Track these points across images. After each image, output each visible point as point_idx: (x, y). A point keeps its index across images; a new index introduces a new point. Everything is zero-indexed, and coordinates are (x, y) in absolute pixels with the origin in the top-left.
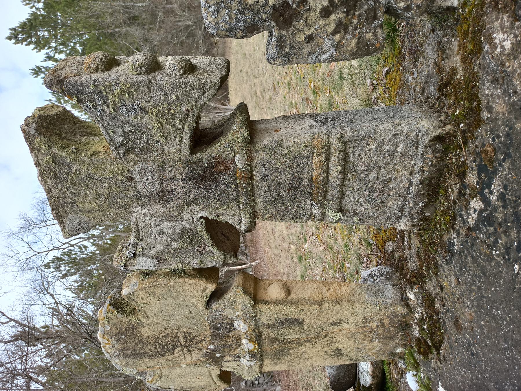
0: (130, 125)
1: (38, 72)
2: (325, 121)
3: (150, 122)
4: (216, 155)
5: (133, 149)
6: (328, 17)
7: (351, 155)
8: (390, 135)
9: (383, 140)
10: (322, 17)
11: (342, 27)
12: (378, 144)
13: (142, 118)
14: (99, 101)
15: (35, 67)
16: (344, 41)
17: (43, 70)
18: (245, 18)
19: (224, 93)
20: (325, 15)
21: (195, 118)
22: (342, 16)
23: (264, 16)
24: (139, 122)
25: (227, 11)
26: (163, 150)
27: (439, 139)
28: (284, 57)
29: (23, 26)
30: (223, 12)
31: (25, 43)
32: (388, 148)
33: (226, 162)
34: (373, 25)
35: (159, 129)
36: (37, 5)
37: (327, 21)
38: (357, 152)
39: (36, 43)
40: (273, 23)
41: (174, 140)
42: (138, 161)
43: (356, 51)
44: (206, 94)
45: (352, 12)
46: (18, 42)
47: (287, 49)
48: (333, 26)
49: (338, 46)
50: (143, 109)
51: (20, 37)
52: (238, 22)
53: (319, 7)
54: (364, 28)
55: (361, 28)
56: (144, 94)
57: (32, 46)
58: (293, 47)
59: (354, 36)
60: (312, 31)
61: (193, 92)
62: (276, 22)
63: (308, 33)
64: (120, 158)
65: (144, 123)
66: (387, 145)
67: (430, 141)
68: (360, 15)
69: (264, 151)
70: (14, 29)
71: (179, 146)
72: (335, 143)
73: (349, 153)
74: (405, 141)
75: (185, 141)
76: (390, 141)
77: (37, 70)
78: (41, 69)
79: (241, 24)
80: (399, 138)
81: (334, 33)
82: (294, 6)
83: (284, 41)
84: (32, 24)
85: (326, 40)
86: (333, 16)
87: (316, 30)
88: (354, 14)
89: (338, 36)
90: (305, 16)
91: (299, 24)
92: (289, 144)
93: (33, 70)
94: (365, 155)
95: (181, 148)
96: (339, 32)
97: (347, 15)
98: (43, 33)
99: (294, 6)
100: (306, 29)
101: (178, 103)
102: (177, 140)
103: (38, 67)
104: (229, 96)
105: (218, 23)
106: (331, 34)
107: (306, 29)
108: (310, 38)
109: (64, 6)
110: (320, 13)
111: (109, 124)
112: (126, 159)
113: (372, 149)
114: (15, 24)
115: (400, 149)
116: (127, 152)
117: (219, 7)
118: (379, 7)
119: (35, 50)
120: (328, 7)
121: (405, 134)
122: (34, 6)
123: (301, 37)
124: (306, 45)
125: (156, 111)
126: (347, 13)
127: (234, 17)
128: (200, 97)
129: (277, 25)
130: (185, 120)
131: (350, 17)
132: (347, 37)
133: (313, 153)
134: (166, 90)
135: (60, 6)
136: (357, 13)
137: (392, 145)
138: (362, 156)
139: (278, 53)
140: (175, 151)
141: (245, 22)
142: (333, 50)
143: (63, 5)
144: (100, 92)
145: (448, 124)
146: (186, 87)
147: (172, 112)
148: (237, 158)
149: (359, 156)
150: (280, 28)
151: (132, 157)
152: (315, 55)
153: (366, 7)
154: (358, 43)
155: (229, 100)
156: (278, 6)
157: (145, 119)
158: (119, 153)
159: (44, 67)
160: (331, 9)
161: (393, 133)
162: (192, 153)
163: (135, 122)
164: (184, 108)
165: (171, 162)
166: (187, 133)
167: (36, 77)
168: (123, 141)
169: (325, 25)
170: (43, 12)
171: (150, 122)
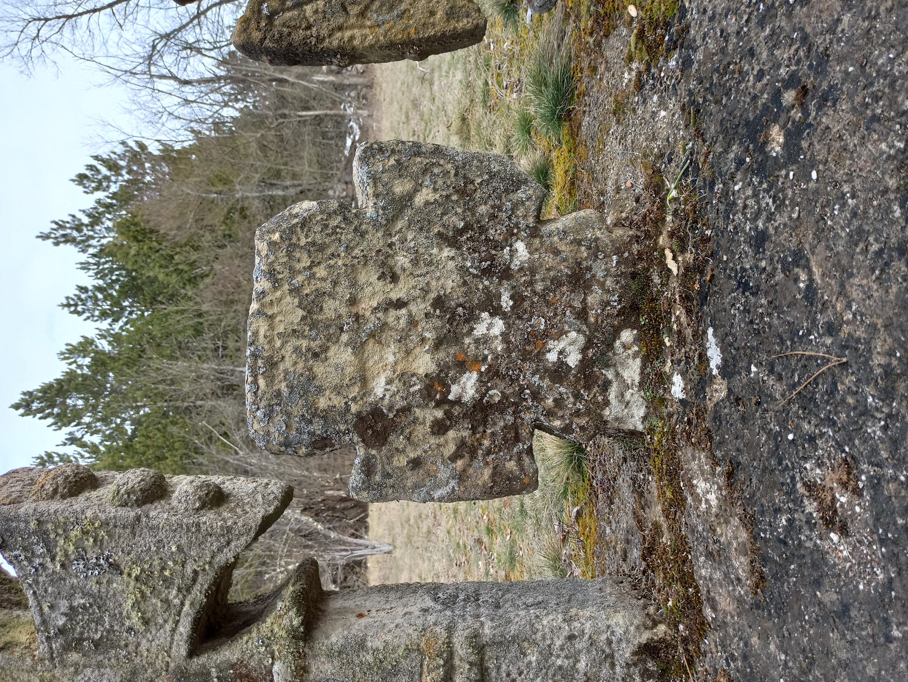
0: (84, 595)
1: (46, 461)
2: (450, 602)
3: (124, 591)
4: (238, 659)
5: (80, 640)
6: (444, 434)
7: (494, 674)
8: (562, 638)
9: (549, 646)
10: (433, 433)
11: (465, 450)
12: (541, 653)
13: (109, 582)
14: (40, 550)
15: (43, 454)
16: (471, 471)
17: (56, 459)
18: (311, 428)
19: (361, 513)
20: (439, 431)
21: (206, 586)
22: (466, 434)
23: (343, 428)
24: (103, 590)
25: (284, 417)
26: (138, 645)
27: (649, 650)
28: (373, 490)
29: (47, 390)
30: (279, 418)
31: (39, 415)
32: (559, 662)
33: (254, 674)
34: (515, 450)
35: (136, 605)
36: (80, 361)
37: (442, 439)
38: (504, 667)
39: (58, 415)
40: (356, 438)
41: (162, 626)
42: (85, 666)
43: (492, 487)
44: (233, 544)
45: (481, 429)
46: (29, 411)
47: (378, 478)
48: (451, 448)
49: (462, 477)
50: (115, 567)
51: (35, 406)
52: (300, 434)
53: (429, 419)
54: (501, 454)
55: (497, 453)
56: (122, 540)
57: (50, 420)
58: (388, 475)
59: (487, 463)
60: (419, 452)
61: (209, 539)
62: (362, 435)
63: (412, 455)
64: (52, 659)
65: (111, 592)
66: (558, 656)
67: (634, 654)
68: (493, 434)
69: (330, 656)
70: (30, 394)
71: (169, 639)
72: (461, 650)
73: (488, 668)
74: (588, 651)
75: (181, 629)
76: (562, 649)
77: (46, 458)
78: (53, 457)
79: (305, 437)
80: (580, 645)
81: (454, 458)
82: (391, 415)
83: (374, 465)
84: (62, 387)
85: (442, 467)
86: (451, 434)
87: (426, 452)
88: (485, 432)
89: (460, 463)
90: (408, 431)
91: (399, 441)
92: (378, 644)
93: (38, 458)
94: (520, 675)
95: (171, 643)
96: (462, 457)
97: (474, 433)
99: (391, 415)
100: (409, 449)
101: (179, 558)
102: (168, 627)
103: (49, 456)
104: (368, 520)
105: (268, 433)
106: (449, 458)
107: (409, 449)
108: (416, 463)
109: (123, 365)
110: (432, 427)
111: (46, 591)
112: (62, 661)
113: (530, 662)
114: (34, 385)
115: (582, 665)
116: (66, 648)
117: (272, 411)
118: (522, 424)
119: (53, 427)
120: (443, 420)
121: (587, 636)
122: (75, 362)
123: (401, 461)
124: (409, 473)
125: (136, 571)
126: (474, 430)
127: (295, 426)
128: (220, 550)
129: (363, 441)
130: (188, 590)
131: (478, 436)
132: (475, 464)
133: (421, 666)
134: (161, 535)
135: (116, 364)
136: (489, 431)
137: (567, 657)
138: (514, 676)
139: (363, 483)
140: (161, 648)
141: (312, 434)
142: (453, 483)
143: (121, 362)
144: (46, 532)
145: (660, 622)
146: (198, 530)
147: (167, 573)
148: (276, 668)
149: (508, 675)
150: (367, 445)
151: (74, 657)
152: (425, 490)
153: (502, 424)
154: (494, 475)
155: (367, 528)
156: (365, 413)
157: (115, 585)
158: (51, 648)
159: (59, 455)
160: (448, 423)
161: (565, 634)
162: (192, 653)
163: (95, 588)
164: (189, 570)
165: (150, 671)
166: (188, 614)
168: (65, 625)
169: (439, 446)
170: (86, 371)
171: (124, 591)
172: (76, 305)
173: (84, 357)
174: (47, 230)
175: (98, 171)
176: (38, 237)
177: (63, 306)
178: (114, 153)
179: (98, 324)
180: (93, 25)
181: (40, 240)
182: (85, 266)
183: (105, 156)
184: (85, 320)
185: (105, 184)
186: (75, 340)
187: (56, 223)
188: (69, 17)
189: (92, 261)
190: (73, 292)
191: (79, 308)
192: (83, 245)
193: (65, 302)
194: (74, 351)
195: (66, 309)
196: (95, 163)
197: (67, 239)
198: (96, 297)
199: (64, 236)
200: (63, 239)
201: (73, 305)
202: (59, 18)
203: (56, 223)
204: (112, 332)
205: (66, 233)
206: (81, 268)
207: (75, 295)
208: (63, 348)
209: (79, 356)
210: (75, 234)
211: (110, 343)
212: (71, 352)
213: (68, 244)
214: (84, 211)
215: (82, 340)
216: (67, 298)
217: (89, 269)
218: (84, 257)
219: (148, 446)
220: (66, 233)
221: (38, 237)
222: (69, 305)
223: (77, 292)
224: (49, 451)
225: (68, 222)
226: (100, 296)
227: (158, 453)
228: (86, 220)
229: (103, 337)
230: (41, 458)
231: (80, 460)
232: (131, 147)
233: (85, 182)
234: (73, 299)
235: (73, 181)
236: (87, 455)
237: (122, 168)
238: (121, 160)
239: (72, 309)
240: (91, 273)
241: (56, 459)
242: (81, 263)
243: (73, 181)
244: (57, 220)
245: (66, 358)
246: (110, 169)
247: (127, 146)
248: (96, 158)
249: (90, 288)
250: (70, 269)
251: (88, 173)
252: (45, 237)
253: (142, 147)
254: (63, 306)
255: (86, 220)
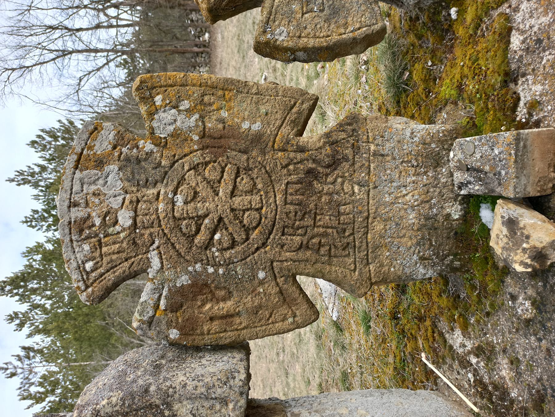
1: (14, 318)
15: (12, 313)
31: (10, 295)
36: (35, 257)
57: (17, 298)
70: (4, 282)
77: (13, 315)
93: (9, 316)
98: (33, 285)
103: (16, 314)
119: (20, 302)
122: (32, 258)
167: (10, 323)
172: (31, 221)
173: (38, 254)
174: (12, 176)
175: (44, 139)
176: (7, 180)
177: (23, 222)
178: (54, 128)
179: (46, 234)
180: (42, 70)
181: (8, 182)
182: (36, 197)
183: (48, 130)
184: (37, 230)
185: (48, 147)
186: (32, 244)
187: (18, 172)
188: (28, 67)
189: (41, 194)
190: (29, 213)
191: (33, 224)
192: (36, 185)
193: (24, 220)
194: (30, 252)
195: (25, 224)
196: (42, 134)
197: (26, 182)
198: (44, 216)
199: (23, 179)
200: (22, 182)
201: (28, 221)
202: (21, 68)
203: (18, 172)
204: (54, 238)
205: (25, 178)
206: (35, 199)
207: (31, 215)
208: (25, 250)
209: (35, 255)
210: (30, 178)
211: (53, 245)
212: (29, 252)
213: (26, 185)
214: (35, 165)
215: (36, 244)
216: (26, 217)
217: (39, 199)
218: (36, 192)
219: (79, 315)
220: (25, 178)
221: (7, 180)
222: (27, 222)
223: (32, 214)
224: (16, 311)
225: (25, 171)
226: (46, 215)
227: (86, 319)
228: (37, 169)
229: (49, 241)
230: (10, 315)
231: (35, 316)
232: (64, 124)
233: (36, 145)
234: (29, 218)
235: (28, 145)
236: (40, 313)
237: (59, 137)
238: (58, 132)
239: (29, 224)
240: (41, 201)
241: (21, 316)
242: (34, 196)
243: (28, 145)
244: (18, 170)
245: (27, 256)
246: (51, 137)
247: (62, 123)
248: (42, 130)
249: (40, 210)
250: (28, 200)
251: (37, 140)
252: (12, 180)
253: (71, 123)
254: (23, 222)
255: (37, 169)
